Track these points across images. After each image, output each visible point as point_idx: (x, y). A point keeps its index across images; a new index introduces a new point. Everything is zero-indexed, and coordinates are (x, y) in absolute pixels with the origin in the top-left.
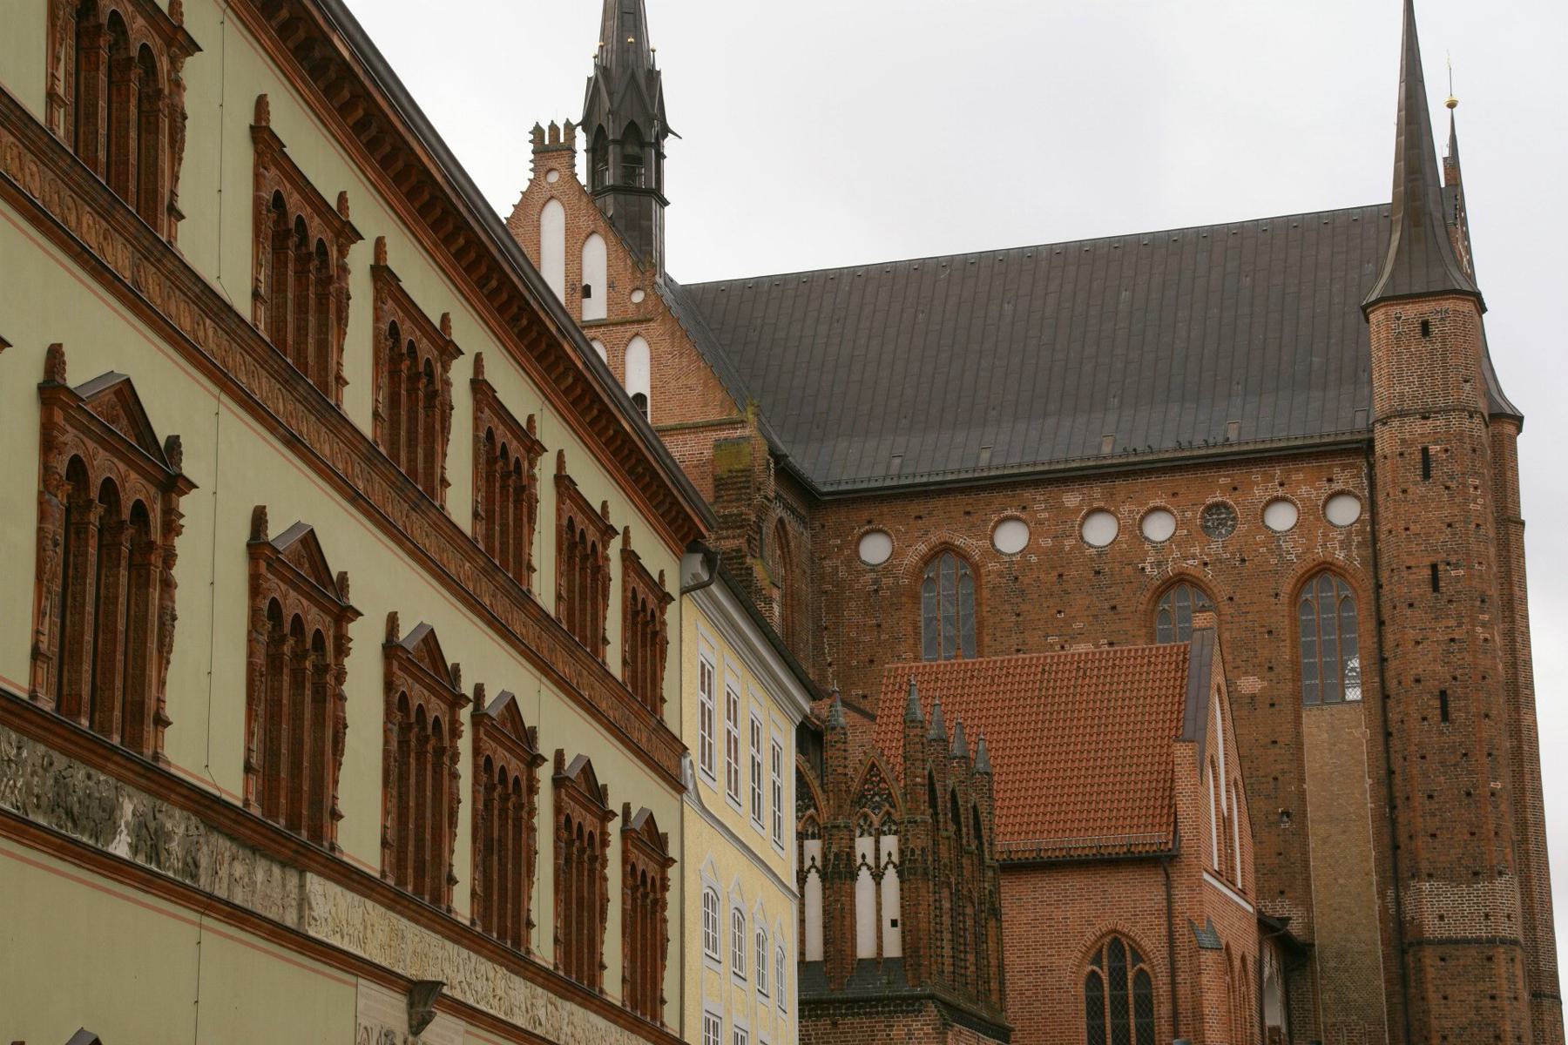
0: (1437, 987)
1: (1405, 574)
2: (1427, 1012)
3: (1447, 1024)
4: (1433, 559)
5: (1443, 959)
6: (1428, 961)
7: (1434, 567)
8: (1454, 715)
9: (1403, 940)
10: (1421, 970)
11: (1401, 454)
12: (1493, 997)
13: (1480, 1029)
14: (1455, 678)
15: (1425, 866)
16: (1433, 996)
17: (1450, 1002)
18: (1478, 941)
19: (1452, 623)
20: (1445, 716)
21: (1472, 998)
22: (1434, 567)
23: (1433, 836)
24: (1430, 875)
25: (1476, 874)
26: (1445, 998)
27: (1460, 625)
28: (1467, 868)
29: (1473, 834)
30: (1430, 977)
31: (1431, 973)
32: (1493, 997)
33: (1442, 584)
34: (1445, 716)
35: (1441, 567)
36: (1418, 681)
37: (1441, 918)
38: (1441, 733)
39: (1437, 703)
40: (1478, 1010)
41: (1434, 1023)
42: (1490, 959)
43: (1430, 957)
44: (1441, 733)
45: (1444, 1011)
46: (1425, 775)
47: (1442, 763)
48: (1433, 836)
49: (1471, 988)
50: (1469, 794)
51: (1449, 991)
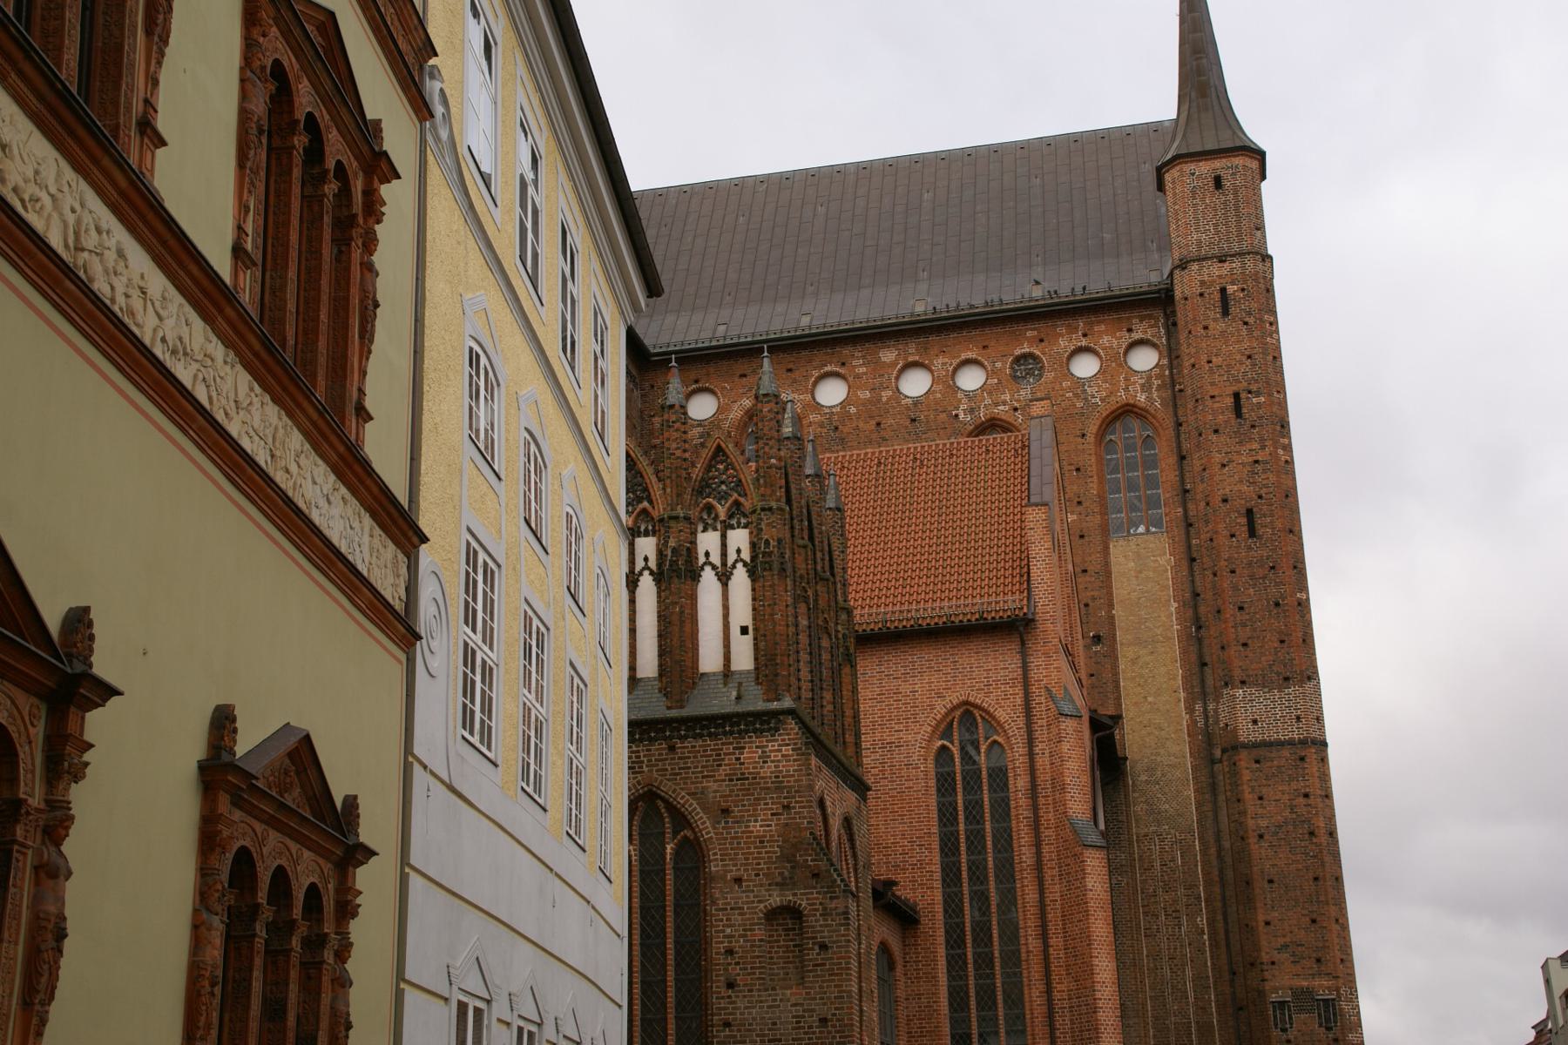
0: (1253, 788)
3: (1263, 823)
5: (1257, 762)
14: (1260, 497)
15: (1238, 674)
17: (1265, 803)
18: (1291, 743)
19: (1255, 446)
20: (1252, 533)
23: (1245, 645)
24: (1243, 682)
25: (1287, 679)
26: (1261, 798)
28: (1278, 674)
34: (1252, 533)
36: (1225, 501)
37: (1255, 722)
38: (1250, 548)
45: (1260, 811)
46: (1235, 588)
47: (1252, 577)
49: (1286, 788)
51: (1264, 790)
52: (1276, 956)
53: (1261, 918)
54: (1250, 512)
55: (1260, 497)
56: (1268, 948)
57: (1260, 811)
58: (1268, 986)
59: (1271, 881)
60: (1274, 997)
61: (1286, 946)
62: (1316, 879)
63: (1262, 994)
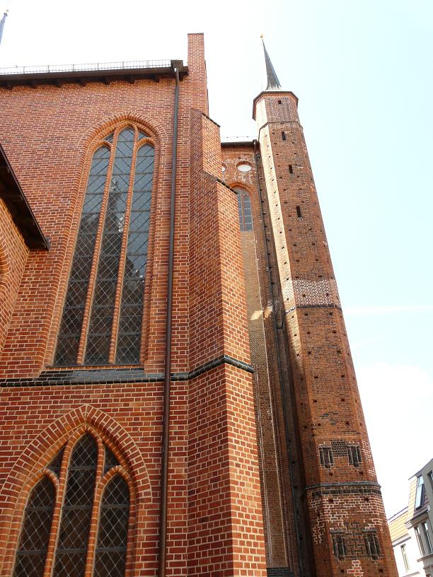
4: (290, 164)
5: (306, 315)
7: (290, 167)
8: (303, 215)
12: (334, 332)
14: (303, 202)
17: (311, 335)
18: (324, 306)
20: (299, 215)
21: (323, 332)
22: (290, 167)
23: (298, 261)
26: (309, 333)
27: (303, 184)
28: (315, 274)
29: (317, 260)
32: (334, 332)
33: (294, 171)
34: (299, 215)
35: (293, 166)
37: (304, 296)
39: (296, 210)
40: (327, 338)
42: (331, 314)
44: (299, 221)
48: (298, 261)
50: (314, 244)
51: (310, 329)
52: (321, 420)
53: (311, 398)
54: (298, 208)
55: (303, 202)
58: (316, 438)
61: (326, 415)
63: (312, 444)
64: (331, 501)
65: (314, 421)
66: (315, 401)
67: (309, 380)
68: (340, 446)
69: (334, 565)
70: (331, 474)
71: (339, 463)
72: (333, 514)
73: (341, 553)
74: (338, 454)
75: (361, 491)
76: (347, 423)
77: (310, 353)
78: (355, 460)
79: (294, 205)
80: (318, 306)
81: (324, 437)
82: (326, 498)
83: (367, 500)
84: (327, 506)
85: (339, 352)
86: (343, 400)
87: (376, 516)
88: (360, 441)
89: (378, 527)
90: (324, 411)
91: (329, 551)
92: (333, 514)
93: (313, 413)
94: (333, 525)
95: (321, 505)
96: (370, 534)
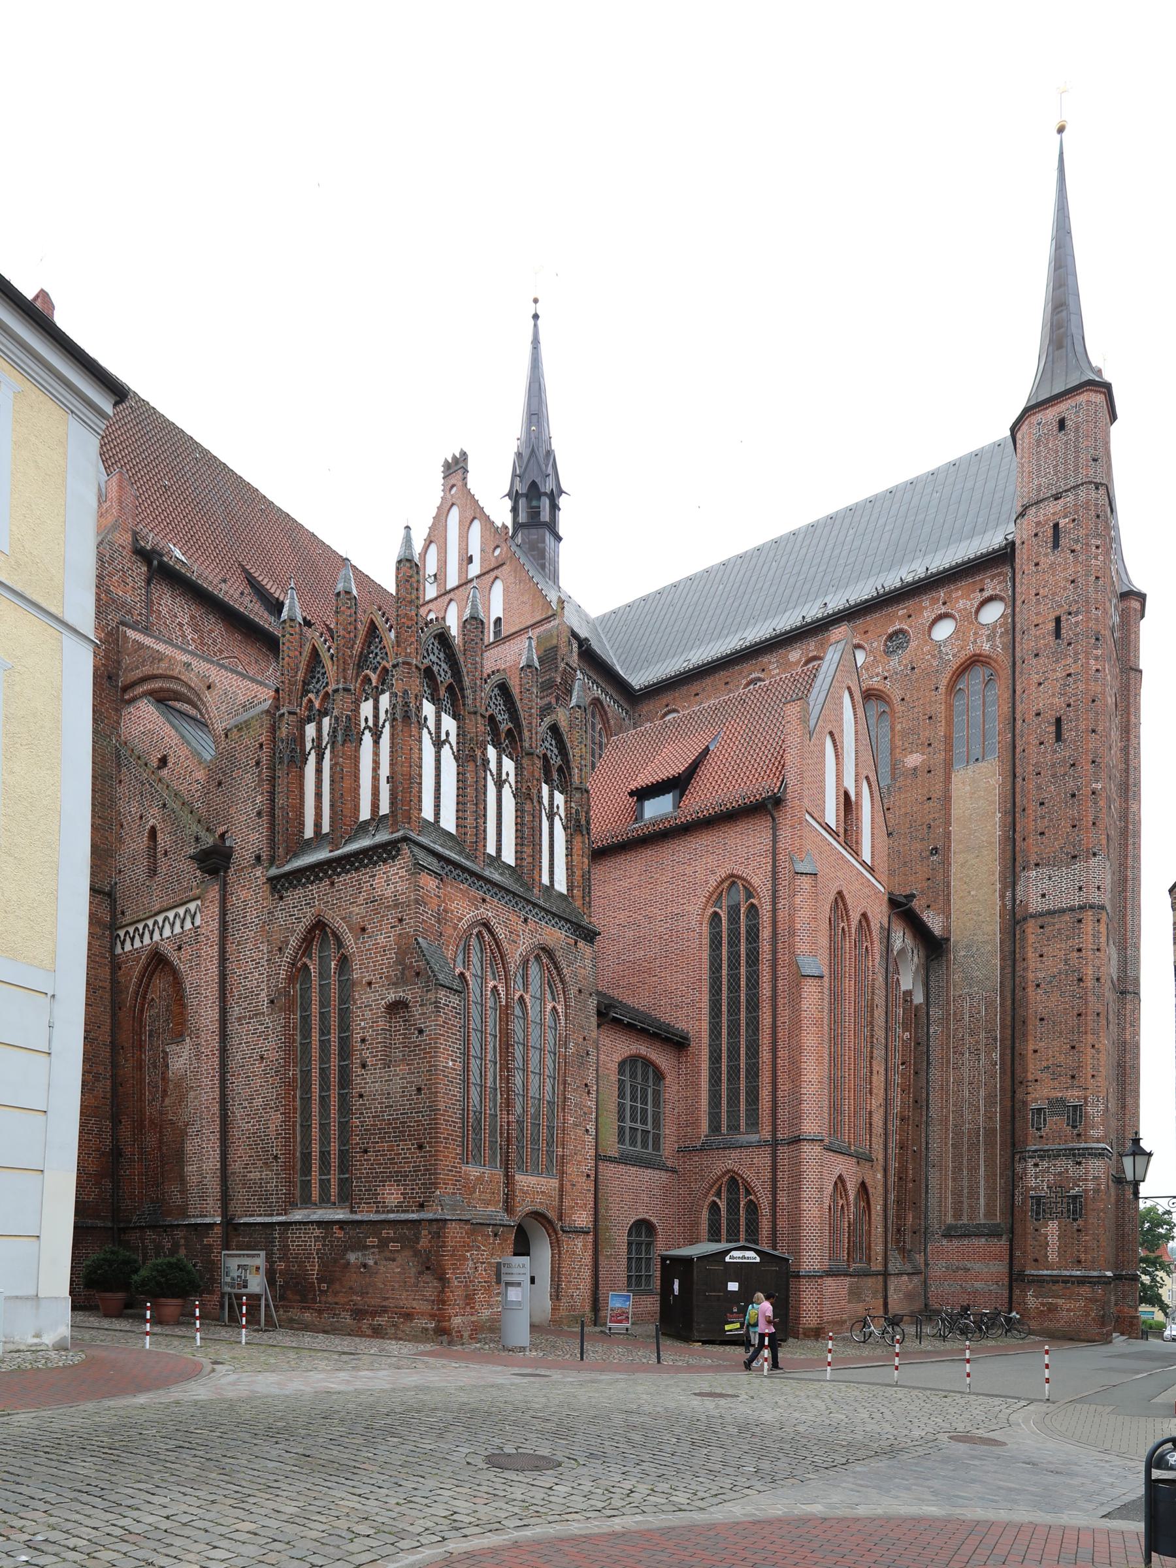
1: (1033, 631)
2: (1025, 969)
3: (1041, 975)
5: (1042, 927)
6: (1030, 930)
9: (1015, 921)
10: (1024, 939)
11: (1036, 535)
13: (1066, 975)
15: (1033, 859)
16: (1031, 955)
23: (1042, 834)
24: (1037, 865)
26: (1041, 956)
30: (1030, 942)
31: (1031, 938)
36: (1038, 714)
41: (1031, 976)
43: (1031, 927)
45: (1039, 966)
46: (1039, 788)
49: (1063, 946)
51: (1045, 949)
52: (1039, 1075)
53: (1031, 1047)
56: (1033, 1068)
57: (1039, 966)
59: (1042, 1019)
60: (1034, 1106)
62: (1079, 1015)
63: (1025, 1103)
64: (1036, 1165)
65: (1030, 1077)
66: (1035, 1051)
67: (1033, 1023)
68: (1058, 1104)
69: (1028, 1225)
70: (1041, 1137)
71: (1056, 1123)
72: (1036, 1178)
73: (1038, 1214)
74: (1053, 1114)
75: (1074, 1155)
76: (1073, 1077)
77: (1038, 986)
78: (1074, 1121)
79: (1050, 716)
80: (1062, 911)
81: (1040, 1094)
82: (1031, 1162)
83: (1079, 1163)
84: (1031, 1170)
85: (1080, 980)
86: (1073, 1047)
87: (1086, 1180)
88: (1086, 1098)
89: (1086, 1191)
90: (1044, 1064)
91: (1026, 1212)
92: (1036, 1178)
93: (1031, 1067)
94: (1034, 1189)
95: (1025, 1169)
96: (1075, 1197)
